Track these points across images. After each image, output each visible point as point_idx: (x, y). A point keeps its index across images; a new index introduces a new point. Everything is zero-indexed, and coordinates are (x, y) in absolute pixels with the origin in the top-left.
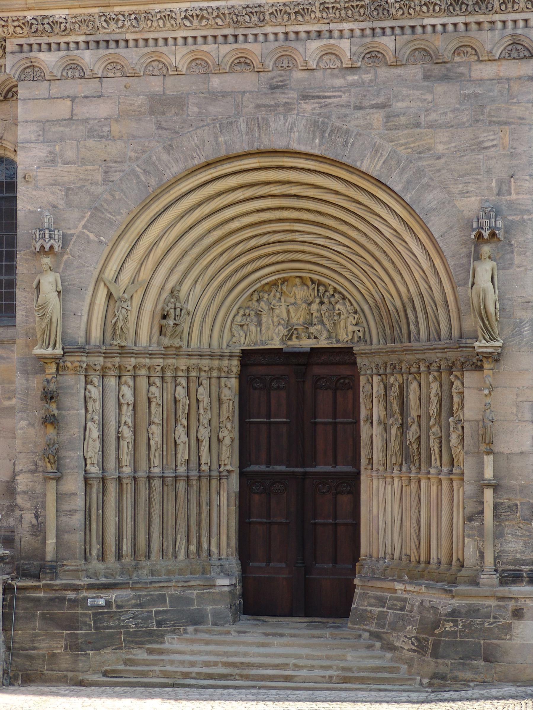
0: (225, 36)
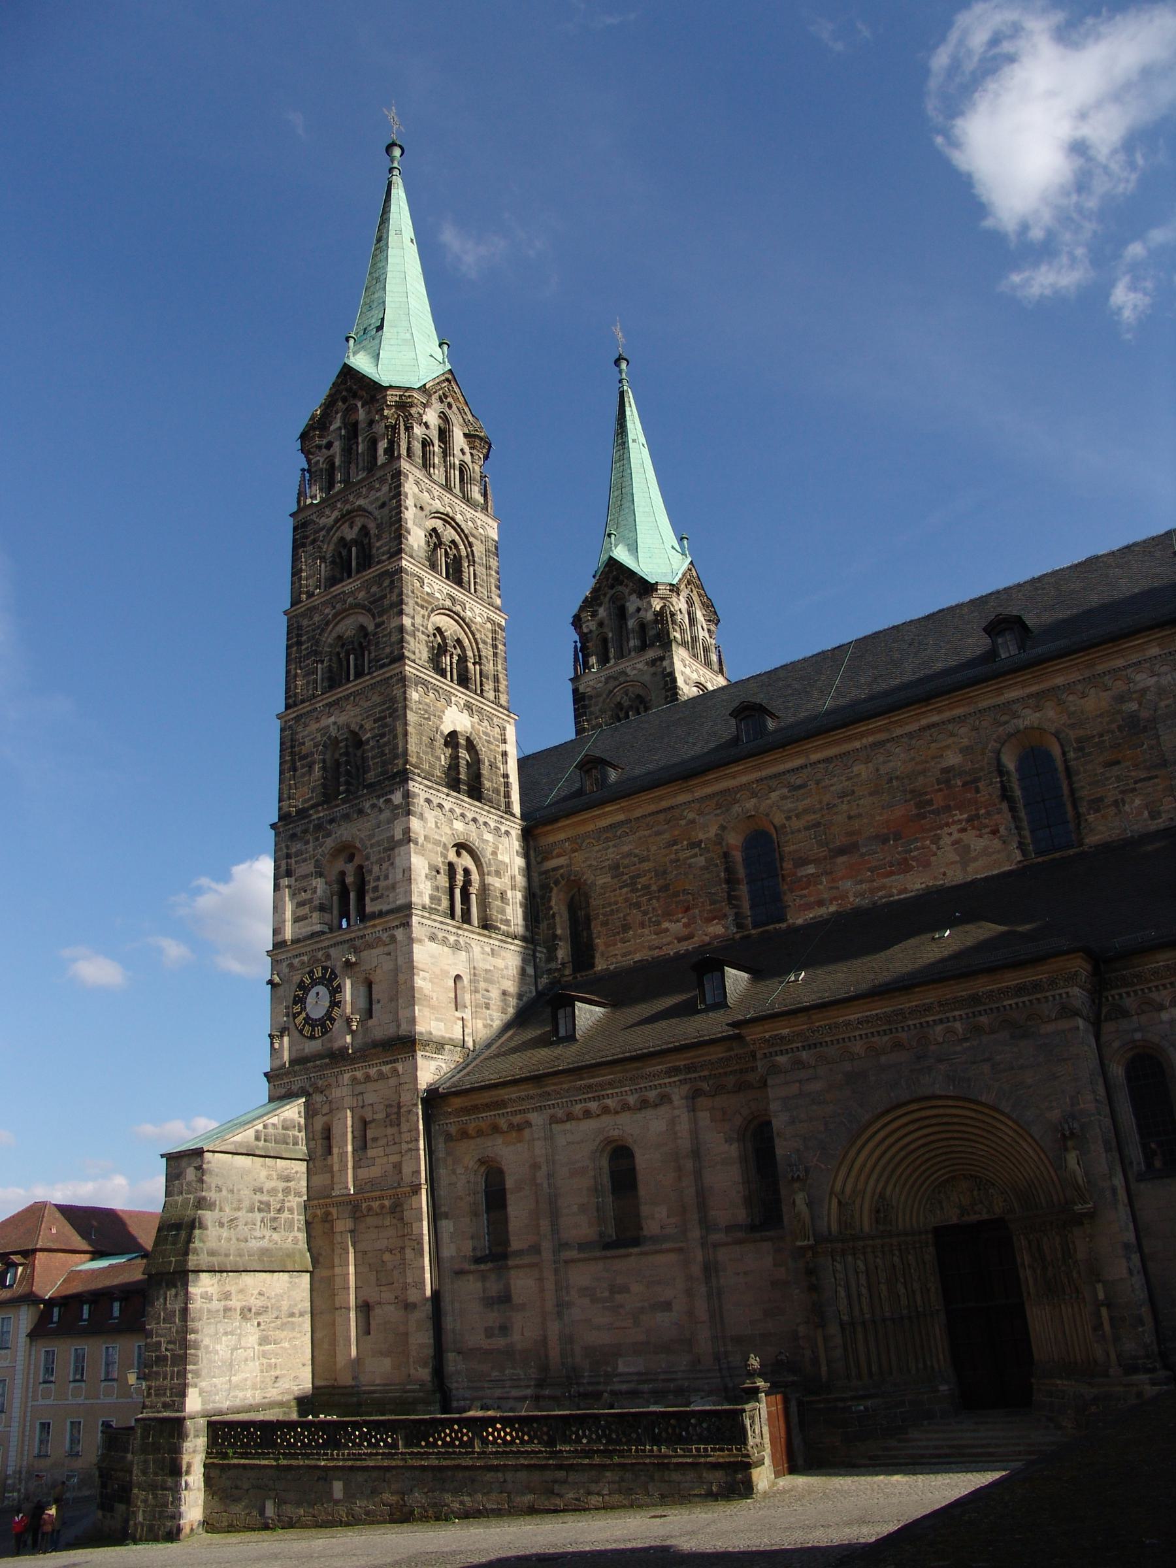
0: (885, 1031)
